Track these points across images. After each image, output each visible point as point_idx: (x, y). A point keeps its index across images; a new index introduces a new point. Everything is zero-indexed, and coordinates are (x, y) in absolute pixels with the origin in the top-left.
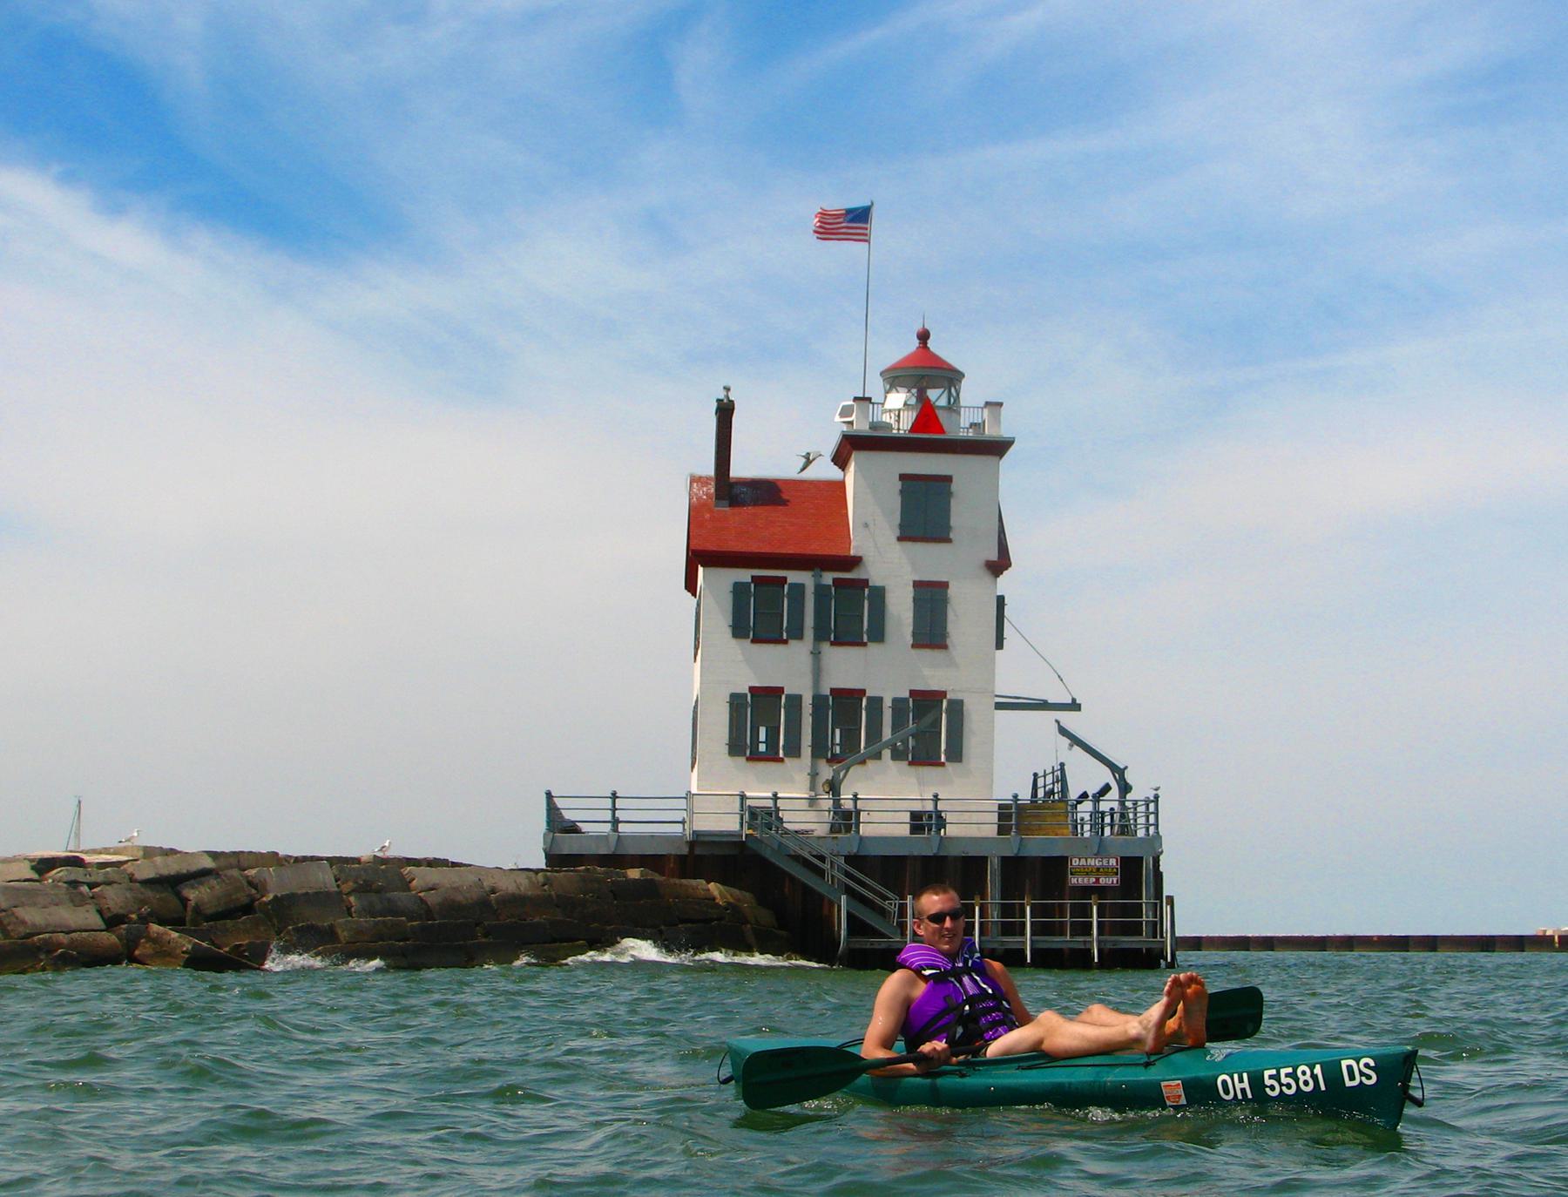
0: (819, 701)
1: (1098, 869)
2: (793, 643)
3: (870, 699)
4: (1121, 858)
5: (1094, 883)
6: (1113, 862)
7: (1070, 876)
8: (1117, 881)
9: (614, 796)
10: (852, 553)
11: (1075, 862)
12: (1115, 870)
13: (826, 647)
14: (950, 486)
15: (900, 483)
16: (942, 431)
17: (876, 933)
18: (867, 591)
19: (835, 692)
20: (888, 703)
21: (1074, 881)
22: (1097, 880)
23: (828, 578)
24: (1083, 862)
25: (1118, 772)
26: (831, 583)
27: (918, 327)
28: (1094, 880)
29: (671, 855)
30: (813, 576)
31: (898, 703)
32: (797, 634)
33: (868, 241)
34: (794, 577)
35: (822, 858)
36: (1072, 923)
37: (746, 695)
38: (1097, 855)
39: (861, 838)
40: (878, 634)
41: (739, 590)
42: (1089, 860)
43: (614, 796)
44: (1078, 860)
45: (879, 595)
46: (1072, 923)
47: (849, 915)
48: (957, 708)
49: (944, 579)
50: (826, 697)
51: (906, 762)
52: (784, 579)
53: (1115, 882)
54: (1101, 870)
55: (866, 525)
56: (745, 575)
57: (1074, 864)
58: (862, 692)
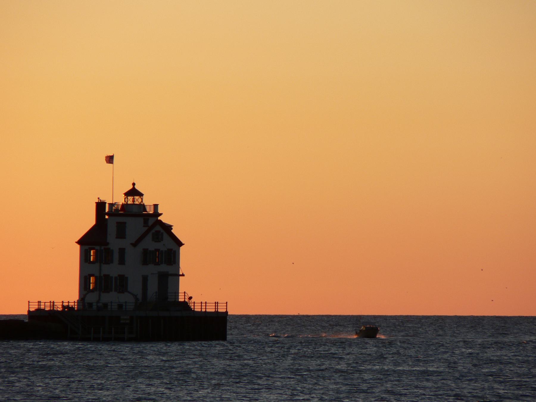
19: (105, 275)
21: (122, 322)
23: (103, 248)
33: (113, 164)
40: (112, 262)
48: (127, 278)
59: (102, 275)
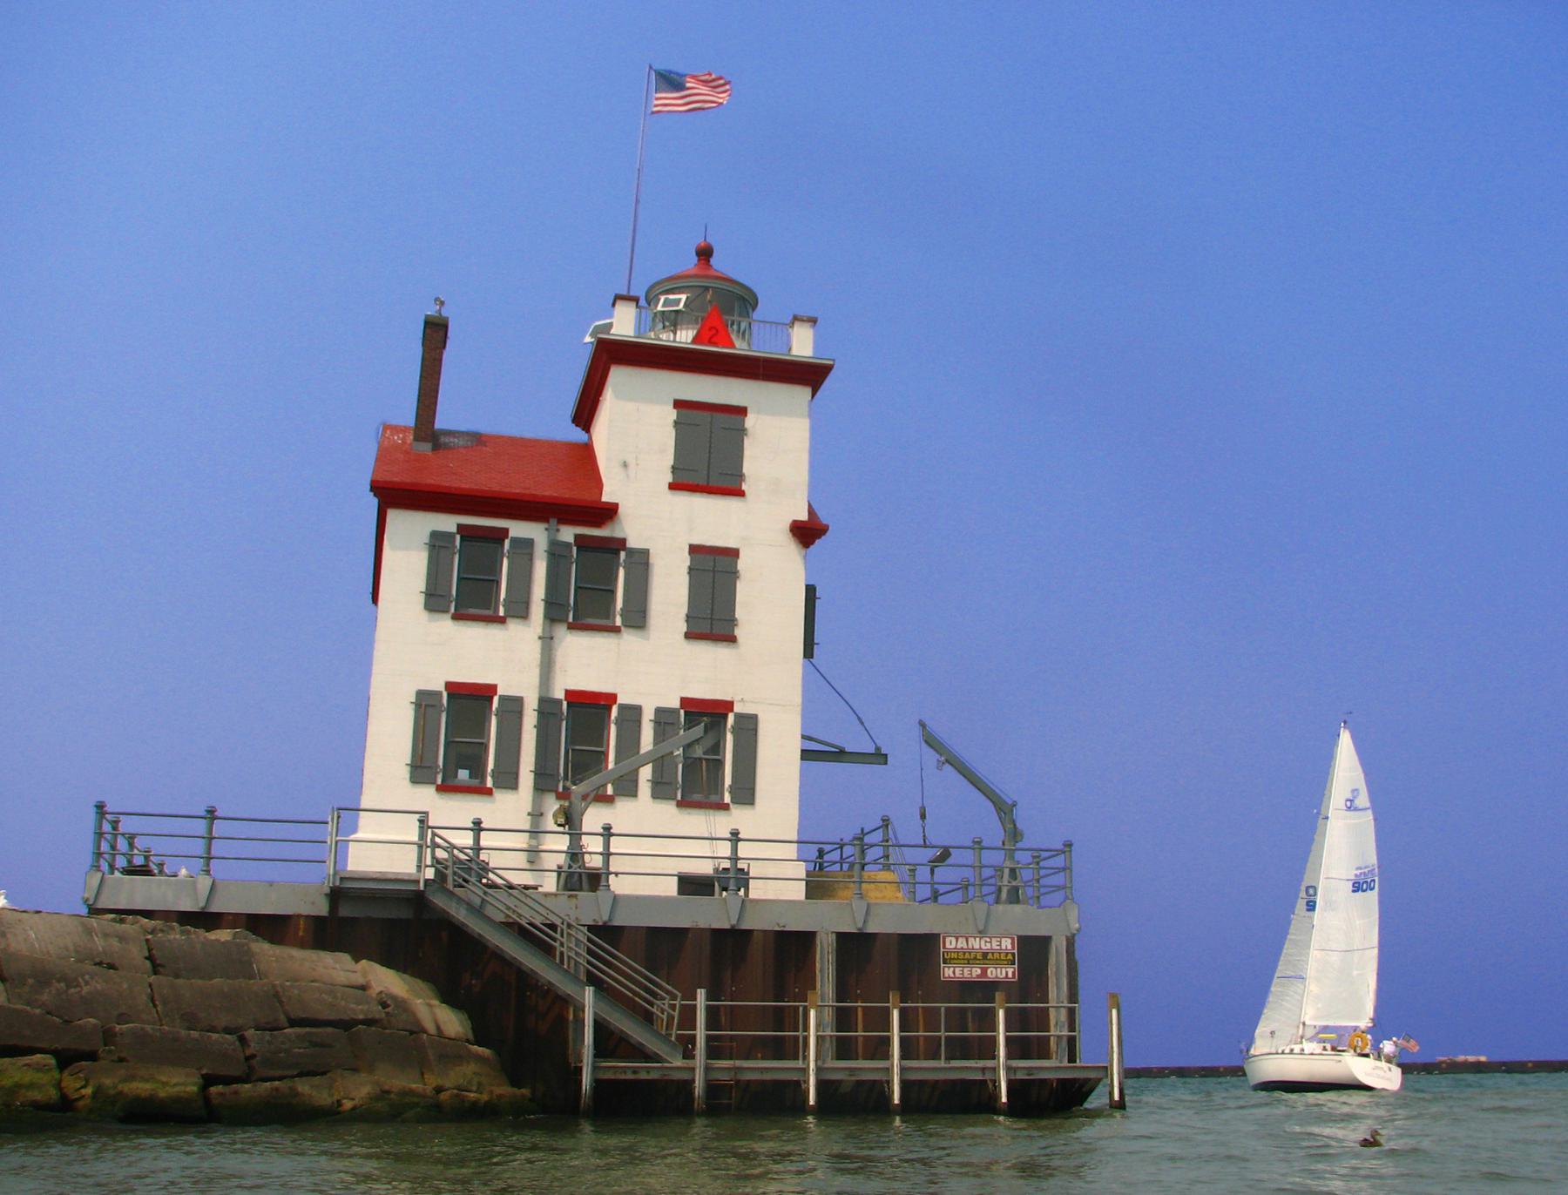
0: (547, 707)
1: (985, 955)
2: (514, 626)
3: (623, 708)
4: (1020, 938)
5: (978, 976)
6: (1007, 944)
7: (942, 965)
8: (1014, 973)
9: (211, 815)
10: (605, 499)
11: (951, 943)
12: (1010, 957)
13: (561, 631)
14: (744, 421)
15: (675, 411)
16: (732, 345)
17: (640, 1053)
18: (623, 554)
19: (576, 698)
20: (648, 716)
21: (948, 972)
22: (984, 971)
23: (568, 534)
24: (962, 943)
25: (1004, 809)
26: (571, 540)
27: (699, 241)
28: (979, 971)
29: (299, 916)
30: (546, 529)
31: (664, 718)
32: (520, 610)
34: (518, 529)
35: (553, 927)
36: (940, 1037)
37: (439, 694)
38: (982, 933)
39: (616, 898)
41: (437, 542)
42: (971, 940)
43: (211, 815)
44: (954, 940)
45: (641, 560)
46: (940, 1037)
47: (599, 1025)
49: (731, 544)
50: (559, 702)
51: (674, 803)
52: (506, 531)
53: (1010, 975)
54: (990, 956)
55: (625, 465)
56: (448, 523)
57: (948, 946)
58: (612, 698)
59: (559, 694)
